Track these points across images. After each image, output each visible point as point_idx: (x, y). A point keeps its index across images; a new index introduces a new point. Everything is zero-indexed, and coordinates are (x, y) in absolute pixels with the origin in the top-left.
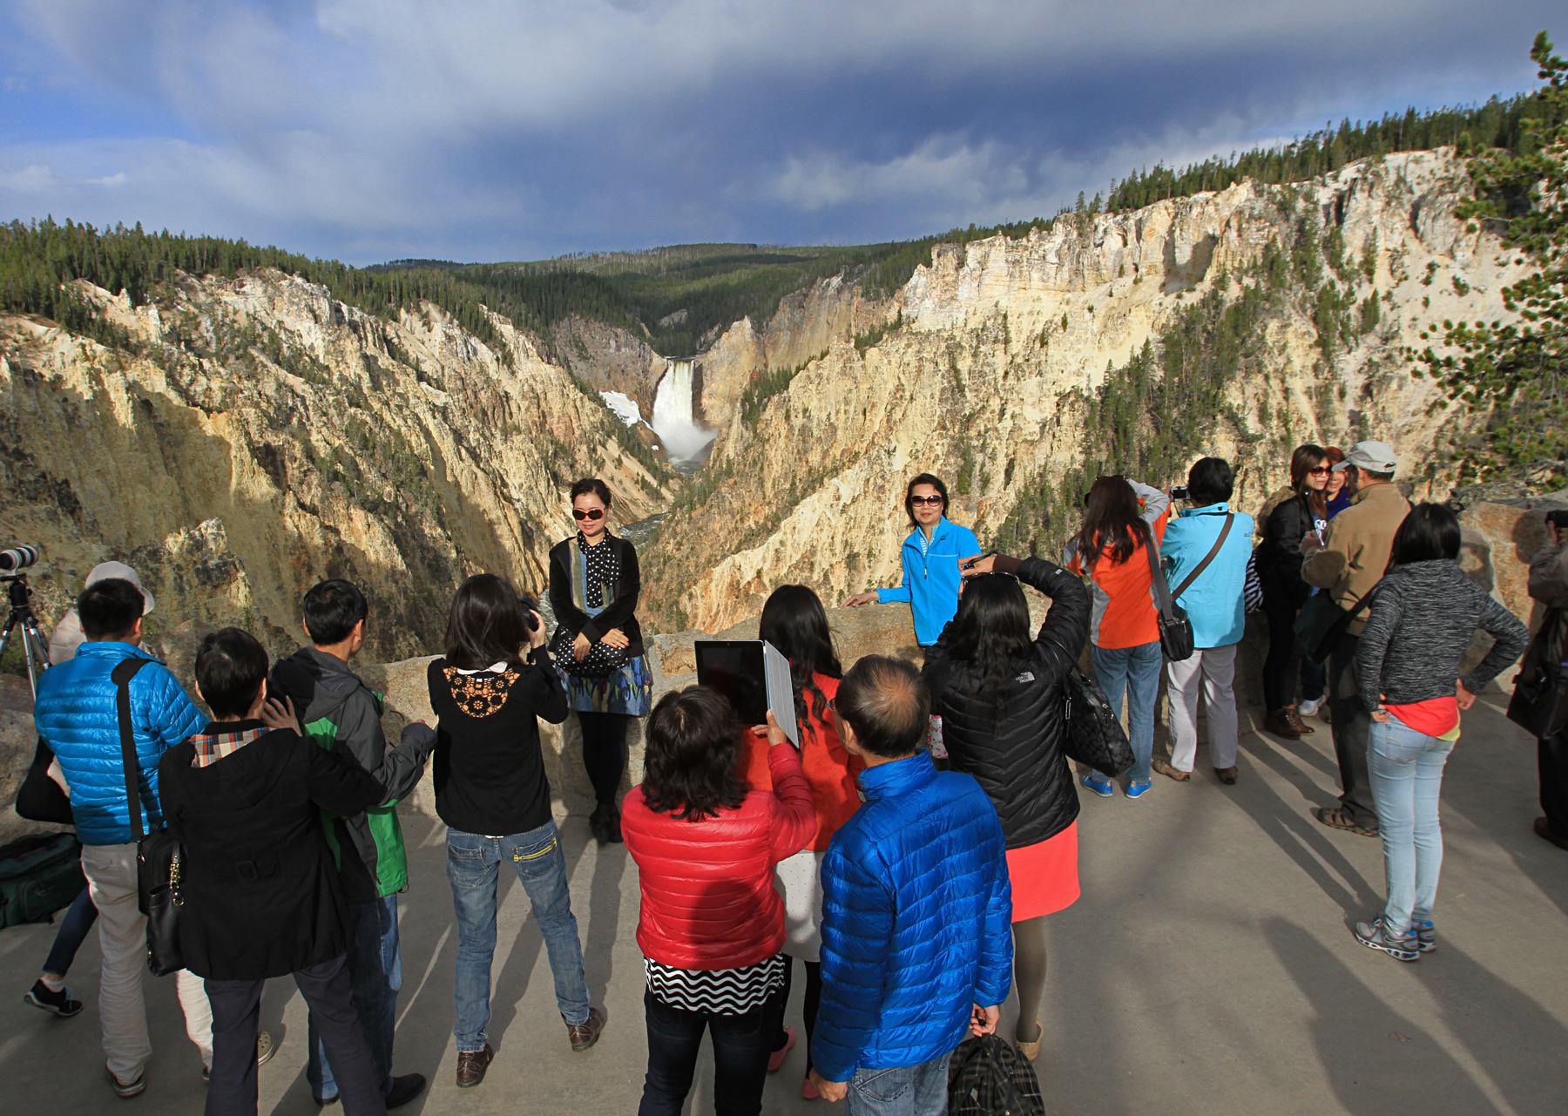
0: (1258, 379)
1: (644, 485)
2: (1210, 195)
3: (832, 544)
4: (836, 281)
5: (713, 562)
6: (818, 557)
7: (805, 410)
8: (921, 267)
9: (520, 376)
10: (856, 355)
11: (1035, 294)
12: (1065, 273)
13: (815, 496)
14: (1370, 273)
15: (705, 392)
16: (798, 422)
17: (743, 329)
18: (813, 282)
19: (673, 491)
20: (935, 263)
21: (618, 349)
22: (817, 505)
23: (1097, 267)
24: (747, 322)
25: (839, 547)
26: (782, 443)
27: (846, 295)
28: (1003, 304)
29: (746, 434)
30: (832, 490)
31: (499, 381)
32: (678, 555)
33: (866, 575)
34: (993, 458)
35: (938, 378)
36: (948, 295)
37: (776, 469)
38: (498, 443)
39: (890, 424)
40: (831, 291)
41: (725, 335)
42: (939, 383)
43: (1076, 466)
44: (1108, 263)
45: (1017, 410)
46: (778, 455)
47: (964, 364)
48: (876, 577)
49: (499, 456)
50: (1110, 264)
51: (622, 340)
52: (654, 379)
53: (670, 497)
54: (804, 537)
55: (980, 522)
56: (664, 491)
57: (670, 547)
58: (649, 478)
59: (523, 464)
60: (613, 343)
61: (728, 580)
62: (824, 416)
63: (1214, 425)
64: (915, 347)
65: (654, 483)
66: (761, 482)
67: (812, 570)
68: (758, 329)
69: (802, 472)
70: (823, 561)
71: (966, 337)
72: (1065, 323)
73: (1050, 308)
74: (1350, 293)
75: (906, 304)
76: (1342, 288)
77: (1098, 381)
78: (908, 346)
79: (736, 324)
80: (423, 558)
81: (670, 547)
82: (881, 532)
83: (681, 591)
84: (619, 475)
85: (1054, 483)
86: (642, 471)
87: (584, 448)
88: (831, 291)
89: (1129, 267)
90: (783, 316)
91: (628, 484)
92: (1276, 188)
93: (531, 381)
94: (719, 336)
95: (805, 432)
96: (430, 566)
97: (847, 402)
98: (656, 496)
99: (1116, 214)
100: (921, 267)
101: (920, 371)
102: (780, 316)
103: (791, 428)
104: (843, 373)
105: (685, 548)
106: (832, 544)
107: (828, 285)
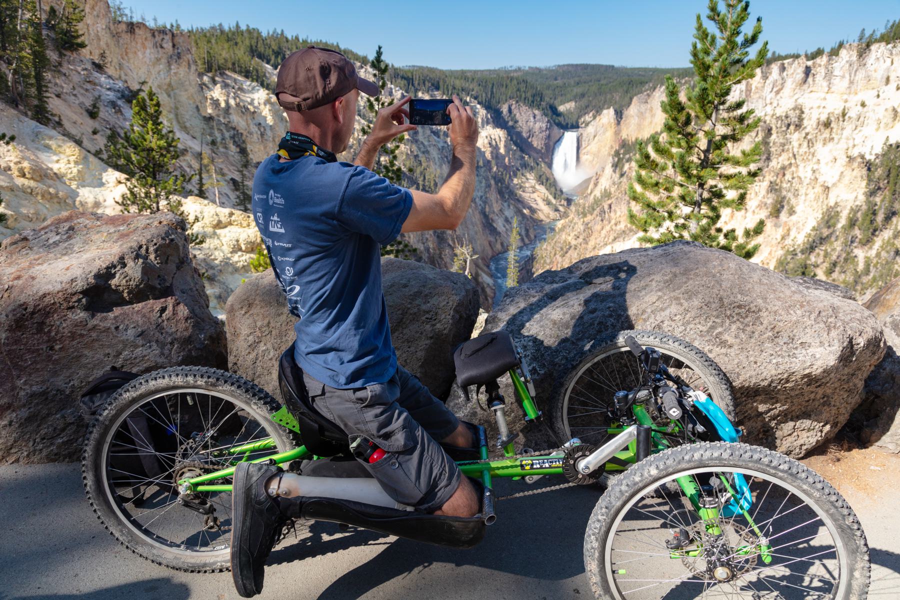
1: (549, 203)
11: (823, 95)
17: (608, 115)
18: (655, 89)
23: (868, 79)
24: (611, 111)
29: (614, 175)
41: (598, 118)
45: (815, 167)
50: (879, 77)
51: (538, 117)
58: (551, 197)
59: (483, 185)
60: (532, 119)
68: (619, 115)
71: (774, 121)
72: (844, 115)
73: (834, 105)
77: (878, 150)
79: (605, 112)
86: (547, 193)
94: (595, 117)
96: (438, 237)
99: (888, 43)
105: (580, 240)
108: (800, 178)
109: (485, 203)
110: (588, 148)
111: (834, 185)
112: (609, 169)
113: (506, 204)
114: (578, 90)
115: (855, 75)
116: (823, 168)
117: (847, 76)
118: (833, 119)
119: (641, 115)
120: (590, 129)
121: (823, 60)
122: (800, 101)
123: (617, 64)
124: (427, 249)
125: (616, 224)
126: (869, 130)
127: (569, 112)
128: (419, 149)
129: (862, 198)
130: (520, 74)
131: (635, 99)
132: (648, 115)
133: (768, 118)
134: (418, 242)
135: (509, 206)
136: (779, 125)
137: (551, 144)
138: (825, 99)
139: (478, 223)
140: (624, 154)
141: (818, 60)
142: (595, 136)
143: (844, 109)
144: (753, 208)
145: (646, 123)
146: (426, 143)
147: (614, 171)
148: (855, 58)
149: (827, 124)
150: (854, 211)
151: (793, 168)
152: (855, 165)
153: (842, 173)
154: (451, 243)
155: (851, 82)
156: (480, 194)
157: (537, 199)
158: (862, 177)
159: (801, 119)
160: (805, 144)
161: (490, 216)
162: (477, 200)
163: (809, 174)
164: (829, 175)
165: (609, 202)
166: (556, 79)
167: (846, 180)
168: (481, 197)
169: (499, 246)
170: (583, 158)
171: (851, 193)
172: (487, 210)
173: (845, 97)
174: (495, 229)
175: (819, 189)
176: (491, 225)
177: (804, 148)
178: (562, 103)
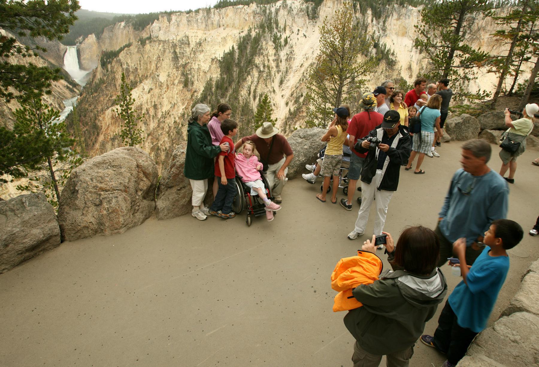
0: (262, 57)
2: (242, 6)
3: (147, 102)
4: (123, 24)
6: (143, 106)
8: (156, 20)
10: (141, 47)
11: (196, 31)
12: (204, 25)
13: (136, 89)
14: (285, 30)
15: (82, 58)
16: (125, 66)
17: (92, 38)
19: (78, 90)
20: (160, 20)
23: (213, 23)
27: (127, 28)
28: (187, 33)
34: (193, 77)
39: (157, 68)
40: (122, 27)
41: (86, 39)
42: (171, 56)
44: (215, 23)
47: (178, 50)
48: (164, 110)
52: (63, 53)
53: (77, 91)
56: (75, 90)
58: (68, 85)
61: (111, 115)
62: (133, 65)
63: (253, 68)
65: (71, 87)
66: (115, 85)
67: (141, 110)
70: (145, 107)
74: (281, 36)
76: (279, 34)
77: (222, 56)
78: (160, 44)
79: (90, 36)
82: (163, 98)
83: (96, 119)
88: (122, 27)
89: (221, 25)
90: (106, 34)
91: (61, 86)
92: (262, 6)
94: (84, 39)
95: (127, 70)
97: (140, 61)
98: (72, 91)
100: (156, 20)
101: (164, 51)
102: (105, 34)
103: (123, 69)
104: (138, 52)
105: (93, 107)
106: (147, 102)
107: (120, 25)
110: (85, 56)
111: (208, 71)
112: (100, 69)
116: (202, 64)
119: (111, 38)
120: (83, 45)
125: (111, 97)
126: (217, 47)
129: (219, 76)
148: (205, 14)
149: (200, 44)
157: (61, 86)
159: (188, 41)
164: (205, 66)
165: (105, 85)
170: (83, 62)
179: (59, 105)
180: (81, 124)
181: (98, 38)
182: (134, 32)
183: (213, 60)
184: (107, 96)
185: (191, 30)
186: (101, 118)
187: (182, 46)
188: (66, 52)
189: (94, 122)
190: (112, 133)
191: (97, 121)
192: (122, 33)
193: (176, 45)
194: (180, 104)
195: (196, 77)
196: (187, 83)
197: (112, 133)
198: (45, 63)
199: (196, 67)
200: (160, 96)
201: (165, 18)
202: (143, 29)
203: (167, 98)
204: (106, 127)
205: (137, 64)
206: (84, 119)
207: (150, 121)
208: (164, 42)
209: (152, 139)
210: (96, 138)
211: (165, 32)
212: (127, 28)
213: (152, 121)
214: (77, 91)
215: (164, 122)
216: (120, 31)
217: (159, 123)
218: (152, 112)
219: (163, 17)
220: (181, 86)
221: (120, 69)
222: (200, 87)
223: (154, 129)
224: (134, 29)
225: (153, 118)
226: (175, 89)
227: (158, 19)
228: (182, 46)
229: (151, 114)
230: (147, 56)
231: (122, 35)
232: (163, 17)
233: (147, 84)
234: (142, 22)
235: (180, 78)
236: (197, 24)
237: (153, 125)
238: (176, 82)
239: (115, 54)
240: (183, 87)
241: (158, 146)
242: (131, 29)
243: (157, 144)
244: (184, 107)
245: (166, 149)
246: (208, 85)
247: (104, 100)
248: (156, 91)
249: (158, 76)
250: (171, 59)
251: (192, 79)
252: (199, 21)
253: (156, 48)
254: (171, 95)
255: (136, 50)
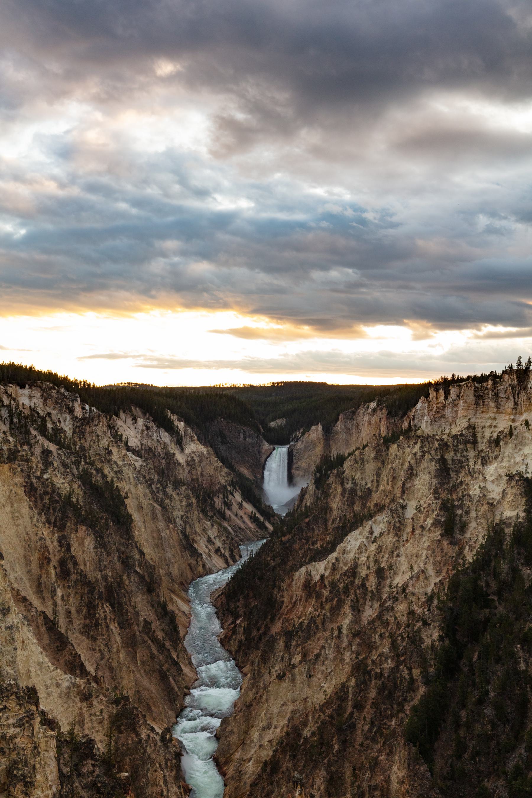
4: (373, 405)
5: (295, 569)
6: (359, 570)
7: (353, 479)
9: (187, 451)
11: (492, 415)
12: (511, 404)
13: (357, 532)
15: (295, 466)
16: (349, 485)
19: (273, 524)
21: (245, 439)
22: (358, 537)
24: (320, 427)
25: (372, 564)
26: (339, 497)
27: (379, 412)
29: (317, 491)
30: (367, 528)
31: (174, 454)
32: (273, 564)
33: (388, 581)
34: (467, 513)
35: (434, 463)
36: (439, 415)
37: (335, 513)
38: (170, 491)
40: (370, 410)
41: (306, 435)
42: (433, 466)
43: (521, 520)
45: (483, 485)
46: (336, 504)
47: (449, 456)
48: (395, 582)
49: (171, 498)
51: (247, 434)
52: (264, 457)
53: (270, 528)
54: (351, 556)
55: (460, 553)
57: (269, 559)
58: (258, 515)
59: (184, 504)
60: (242, 436)
61: (303, 580)
62: (364, 483)
64: (419, 445)
65: (262, 519)
66: (326, 521)
69: (350, 516)
70: (363, 571)
71: (450, 439)
72: (511, 434)
73: (503, 424)
75: (414, 419)
78: (415, 443)
79: (313, 427)
80: (119, 557)
81: (269, 559)
82: (398, 556)
83: (274, 586)
84: (241, 513)
85: (509, 531)
87: (221, 496)
88: (370, 410)
93: (193, 455)
94: (303, 434)
95: (353, 491)
96: (123, 563)
98: (262, 526)
100: (422, 398)
101: (423, 457)
103: (344, 490)
104: (376, 458)
107: (368, 407)
108: (469, 495)
109: (185, 522)
110: (299, 463)
111: (499, 502)
112: (312, 488)
113: (209, 523)
114: (289, 407)
115: (518, 397)
116: (490, 486)
117: (512, 398)
118: (501, 437)
120: (300, 445)
121: (490, 383)
122: (473, 420)
123: (329, 382)
124: (105, 578)
125: (313, 544)
127: (280, 427)
128: (112, 469)
129: (522, 514)
130: (232, 391)
131: (341, 417)
132: (354, 431)
133: (444, 437)
134: (95, 569)
135: (212, 525)
136: (455, 444)
137: (263, 460)
138: (495, 419)
139: (176, 544)
140: (326, 471)
141: (485, 384)
142: (305, 451)
143: (511, 429)
144: (429, 525)
145: (353, 438)
146: (120, 463)
147: (317, 488)
148: (515, 382)
149: (496, 442)
150: (518, 527)
151: (464, 486)
152: (514, 483)
153: (504, 490)
154: (137, 569)
155: (516, 404)
156: (181, 513)
158: (521, 494)
159: (474, 436)
160: (480, 461)
161: (191, 537)
162: (178, 520)
163: (478, 492)
164: (495, 491)
166: (271, 395)
167: (509, 498)
168: (182, 516)
169: (200, 569)
171: (512, 511)
172: (188, 529)
173: (512, 417)
174: (196, 550)
175: (485, 507)
176: (192, 546)
177: (479, 466)
178: (274, 419)
179: (231, 551)
180: (251, 594)
181: (328, 431)
182: (387, 419)
183: (510, 477)
184: (308, 541)
185: (483, 415)
186: (284, 585)
187: (461, 446)
188: (269, 456)
189: (271, 593)
190: (296, 620)
191: (276, 591)
192: (370, 423)
193: (446, 445)
194: (431, 571)
195: (473, 514)
196: (451, 525)
197: (296, 620)
198: (230, 474)
199: (475, 491)
200: (394, 551)
201: (442, 392)
202: (405, 414)
203: (407, 556)
204: (290, 606)
205: (372, 481)
206: (258, 583)
207: (365, 604)
208: (425, 439)
209: (359, 645)
210: (266, 626)
211: (434, 420)
212: (379, 412)
213: (368, 603)
214: (270, 528)
215: (393, 609)
216: (366, 418)
217: (383, 610)
218: (372, 583)
219: (437, 391)
220: (437, 534)
221: (340, 490)
222: (476, 534)
223: (369, 623)
224: (389, 413)
225: (371, 597)
226: (424, 539)
227: (427, 396)
228: (461, 446)
229: (370, 589)
230: (390, 466)
231: (369, 424)
232: (437, 391)
233: (380, 524)
234: (399, 401)
235: (438, 515)
236: (497, 401)
237: (369, 612)
238: (429, 521)
239: (341, 460)
240: (442, 535)
241: (366, 666)
242: (383, 414)
243: (366, 658)
244: (437, 580)
245: (381, 674)
246: (496, 532)
247: (300, 549)
248: (389, 540)
249: (404, 507)
250: (433, 473)
251: (465, 518)
252: (502, 395)
253: (408, 450)
254: (415, 551)
255: (373, 455)
